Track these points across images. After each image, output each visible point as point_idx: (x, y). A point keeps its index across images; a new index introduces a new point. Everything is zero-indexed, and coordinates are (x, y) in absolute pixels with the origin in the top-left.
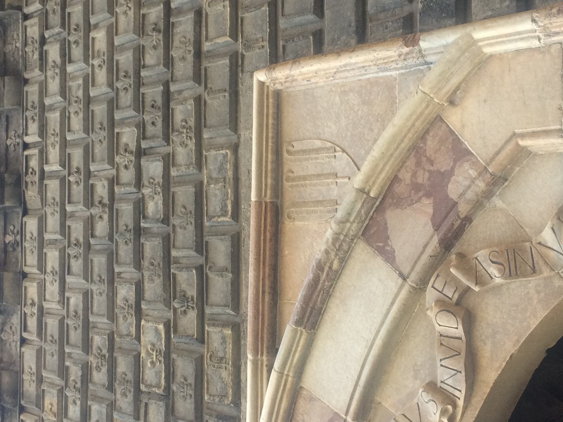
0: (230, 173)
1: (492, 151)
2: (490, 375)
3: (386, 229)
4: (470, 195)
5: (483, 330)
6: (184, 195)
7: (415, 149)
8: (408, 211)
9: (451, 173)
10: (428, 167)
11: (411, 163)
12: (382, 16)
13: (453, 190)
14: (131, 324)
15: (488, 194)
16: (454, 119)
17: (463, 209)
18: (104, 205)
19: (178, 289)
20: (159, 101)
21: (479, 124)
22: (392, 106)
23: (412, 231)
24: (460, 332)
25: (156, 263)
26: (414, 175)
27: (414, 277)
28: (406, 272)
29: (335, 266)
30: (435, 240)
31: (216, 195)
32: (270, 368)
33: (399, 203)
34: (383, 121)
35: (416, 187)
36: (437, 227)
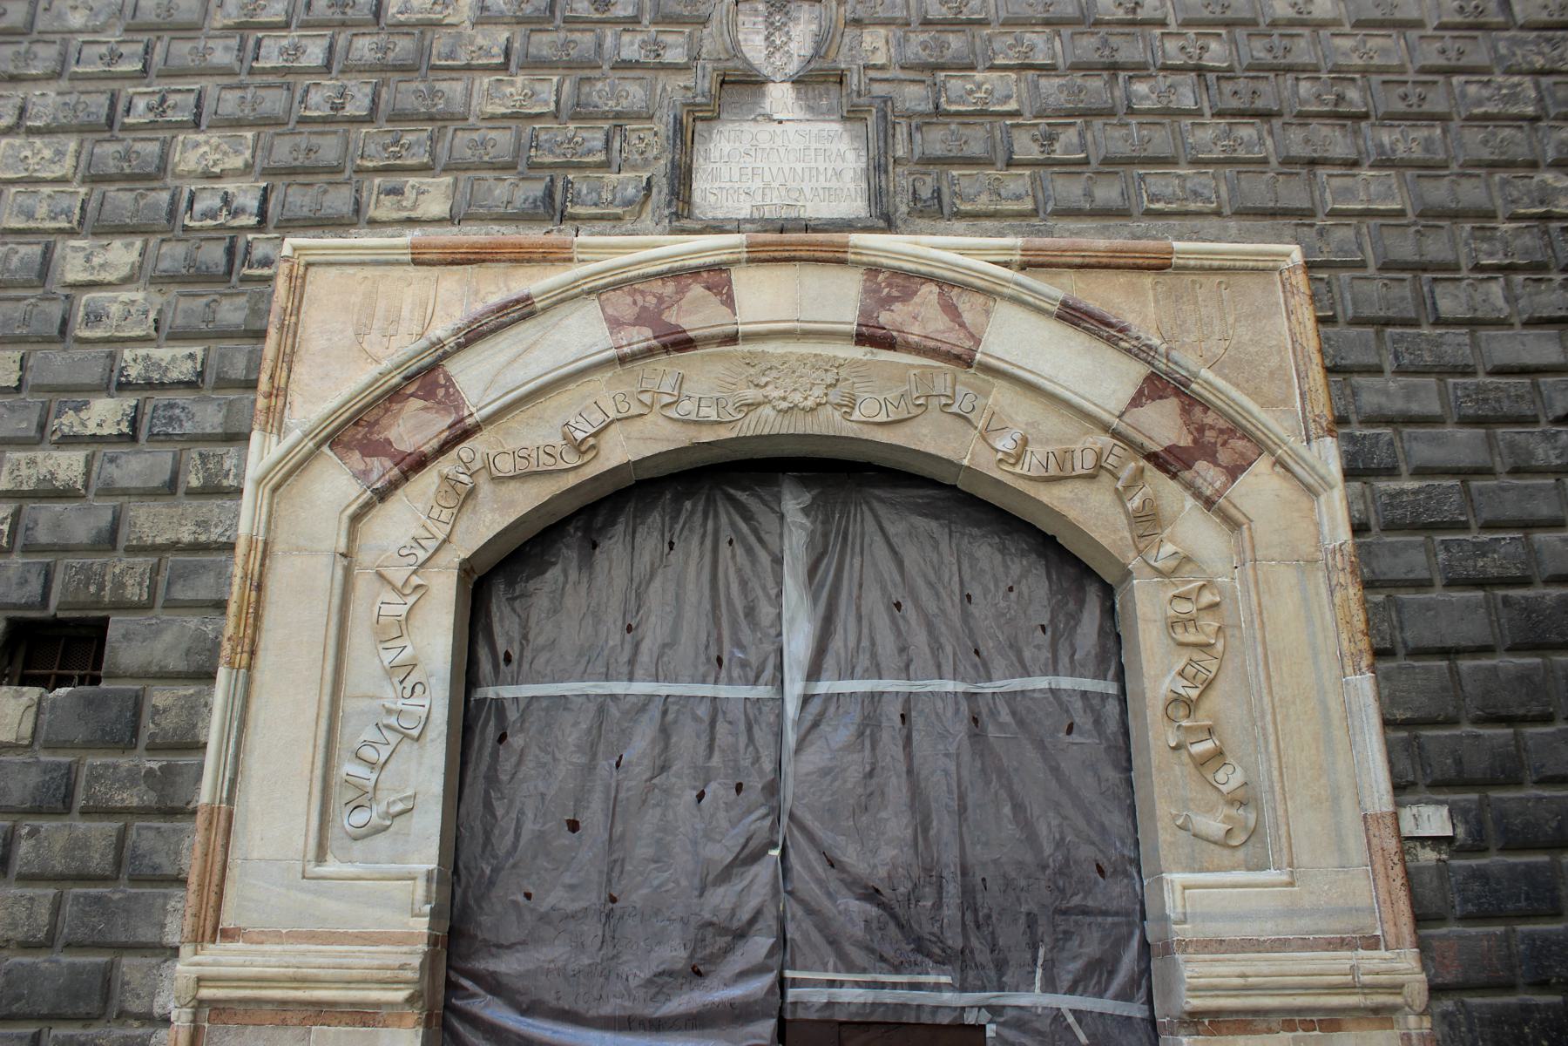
0: (1192, 206)
1: (1237, 502)
3: (1161, 398)
4: (1199, 482)
5: (1080, 488)
6: (1160, 140)
7: (1235, 429)
8: (1179, 421)
9: (1216, 463)
10: (1220, 441)
11: (1222, 424)
12: (1348, 391)
13: (1201, 465)
14: (1007, 56)
15: (1197, 494)
16: (1262, 465)
17: (1187, 475)
18: (1134, 10)
19: (1060, 130)
20: (1260, 104)
21: (1259, 489)
22: (1267, 404)
23: (1162, 425)
24: (1079, 471)
25: (1082, 96)
26: (1212, 427)
27: (1122, 427)
28: (1125, 418)
29: (1123, 344)
30: (1157, 449)
31: (1167, 186)
32: (1006, 265)
33: (1186, 411)
34: (1255, 394)
35: (1201, 429)
36: (1168, 450)
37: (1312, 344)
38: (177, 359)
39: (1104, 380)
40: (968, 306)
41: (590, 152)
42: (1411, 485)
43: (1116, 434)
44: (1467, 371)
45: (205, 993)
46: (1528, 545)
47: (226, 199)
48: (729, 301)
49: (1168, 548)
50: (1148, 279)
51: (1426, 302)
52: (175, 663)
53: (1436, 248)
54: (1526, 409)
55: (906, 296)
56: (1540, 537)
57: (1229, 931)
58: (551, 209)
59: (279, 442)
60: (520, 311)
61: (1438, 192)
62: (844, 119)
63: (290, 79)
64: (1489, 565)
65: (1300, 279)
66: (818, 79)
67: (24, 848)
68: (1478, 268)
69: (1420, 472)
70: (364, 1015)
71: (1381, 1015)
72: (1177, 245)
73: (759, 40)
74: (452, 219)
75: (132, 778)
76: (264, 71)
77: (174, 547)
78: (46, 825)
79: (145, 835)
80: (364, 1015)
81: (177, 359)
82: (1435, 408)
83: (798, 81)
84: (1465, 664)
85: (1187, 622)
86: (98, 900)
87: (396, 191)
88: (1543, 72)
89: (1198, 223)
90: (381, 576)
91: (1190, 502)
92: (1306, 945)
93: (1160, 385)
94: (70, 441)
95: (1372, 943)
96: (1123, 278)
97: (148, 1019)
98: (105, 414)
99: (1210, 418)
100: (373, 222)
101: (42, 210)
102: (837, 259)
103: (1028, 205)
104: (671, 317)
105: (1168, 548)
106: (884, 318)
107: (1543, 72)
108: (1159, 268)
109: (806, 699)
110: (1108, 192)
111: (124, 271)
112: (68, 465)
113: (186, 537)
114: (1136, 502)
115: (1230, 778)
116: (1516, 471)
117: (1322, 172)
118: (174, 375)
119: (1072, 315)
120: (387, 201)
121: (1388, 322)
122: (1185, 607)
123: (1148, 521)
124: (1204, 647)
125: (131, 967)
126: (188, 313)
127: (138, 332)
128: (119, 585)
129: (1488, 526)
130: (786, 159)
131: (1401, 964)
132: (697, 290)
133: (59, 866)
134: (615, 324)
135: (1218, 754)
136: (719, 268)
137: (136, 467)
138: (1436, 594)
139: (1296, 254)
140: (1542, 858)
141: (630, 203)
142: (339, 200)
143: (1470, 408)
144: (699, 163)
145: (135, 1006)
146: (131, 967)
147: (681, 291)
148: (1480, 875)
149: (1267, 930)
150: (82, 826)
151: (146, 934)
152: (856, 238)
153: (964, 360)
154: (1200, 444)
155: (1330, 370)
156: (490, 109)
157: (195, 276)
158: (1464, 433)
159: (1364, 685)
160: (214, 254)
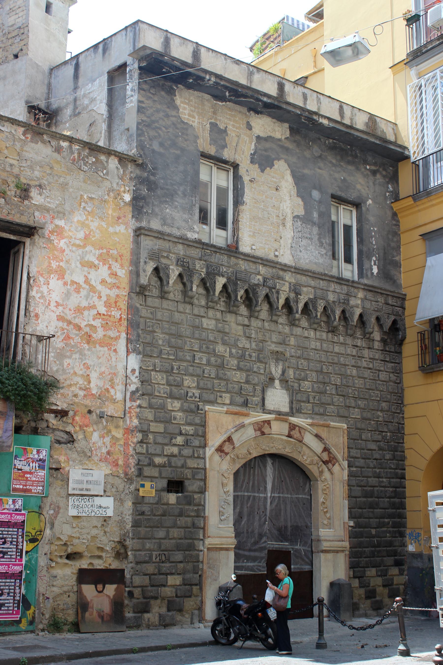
0: (333, 414)
2: (310, 467)
7: (334, 458)
13: (330, 464)
15: (328, 468)
21: (336, 468)
22: (339, 453)
23: (325, 456)
33: (329, 454)
34: (337, 451)
36: (326, 461)
37: (346, 444)
38: (190, 429)
39: (317, 447)
40: (302, 431)
41: (250, 392)
42: (355, 469)
43: (319, 457)
44: (363, 449)
45: (209, 546)
46: (367, 480)
47: (194, 394)
48: (270, 427)
49: (324, 477)
50: (325, 428)
51: (361, 436)
52: (197, 490)
53: (363, 426)
54: (370, 457)
55: (294, 429)
56: (369, 479)
57: (328, 538)
58: (246, 404)
59: (210, 450)
60: (242, 426)
61: (365, 415)
62: (286, 390)
63: (200, 365)
64: (362, 484)
65: (346, 431)
66: (284, 381)
67: (178, 522)
68: (368, 430)
69: (356, 467)
70: (227, 549)
71: (343, 551)
72: (331, 423)
73: (274, 369)
74: (230, 404)
75: (193, 511)
76: (196, 363)
77: (194, 468)
78: (181, 518)
79: (196, 520)
80: (227, 549)
81: (190, 429)
82: (359, 456)
83: (281, 381)
84: (358, 499)
85: (325, 490)
86: (190, 531)
87: (221, 397)
88: (382, 391)
89: (333, 417)
90: (222, 475)
91: (326, 469)
92: (336, 541)
93: (326, 449)
94: (175, 445)
95: (343, 541)
96: (322, 428)
97: (198, 550)
98: (179, 440)
99: (331, 456)
100: (218, 403)
101: (162, 392)
102: (286, 421)
103: (311, 412)
104: (263, 430)
105: (324, 477)
106: (291, 433)
107: (382, 391)
108: (327, 427)
109: (271, 496)
110: (322, 410)
111: (178, 408)
112: (175, 450)
113: (196, 467)
114: (320, 470)
115: (328, 515)
116: (368, 468)
117: (351, 409)
118: (190, 433)
119: (317, 436)
120: (220, 398)
121: (355, 440)
122: (325, 487)
123: (321, 472)
124: (326, 494)
125: (196, 542)
126: (190, 419)
127: (182, 423)
128: (187, 475)
129: (363, 477)
130: (278, 398)
131: (347, 544)
132: (266, 424)
133: (184, 525)
134: (255, 430)
135: (327, 511)
136: (269, 421)
137: (187, 452)
138: (355, 488)
139: (345, 426)
140: (362, 529)
141: (256, 405)
142: (212, 397)
143: (363, 456)
144: (266, 397)
145: (197, 549)
146: (196, 542)
147: (264, 424)
148: (356, 532)
149: (331, 538)
150: (186, 519)
151: (197, 537)
152: (291, 418)
153: (301, 441)
154: (330, 461)
155: (348, 448)
156: (234, 380)
157: (192, 411)
158: (362, 461)
159: (346, 502)
160: (193, 406)
